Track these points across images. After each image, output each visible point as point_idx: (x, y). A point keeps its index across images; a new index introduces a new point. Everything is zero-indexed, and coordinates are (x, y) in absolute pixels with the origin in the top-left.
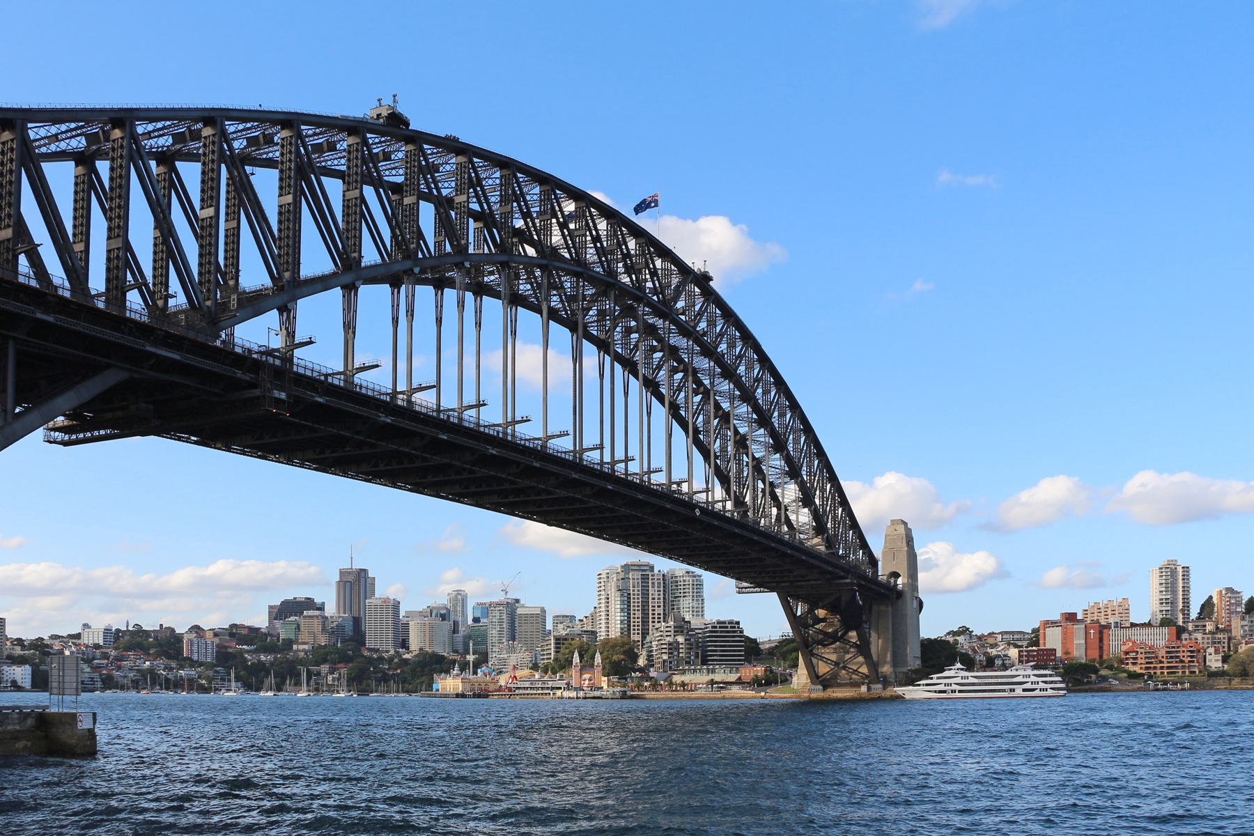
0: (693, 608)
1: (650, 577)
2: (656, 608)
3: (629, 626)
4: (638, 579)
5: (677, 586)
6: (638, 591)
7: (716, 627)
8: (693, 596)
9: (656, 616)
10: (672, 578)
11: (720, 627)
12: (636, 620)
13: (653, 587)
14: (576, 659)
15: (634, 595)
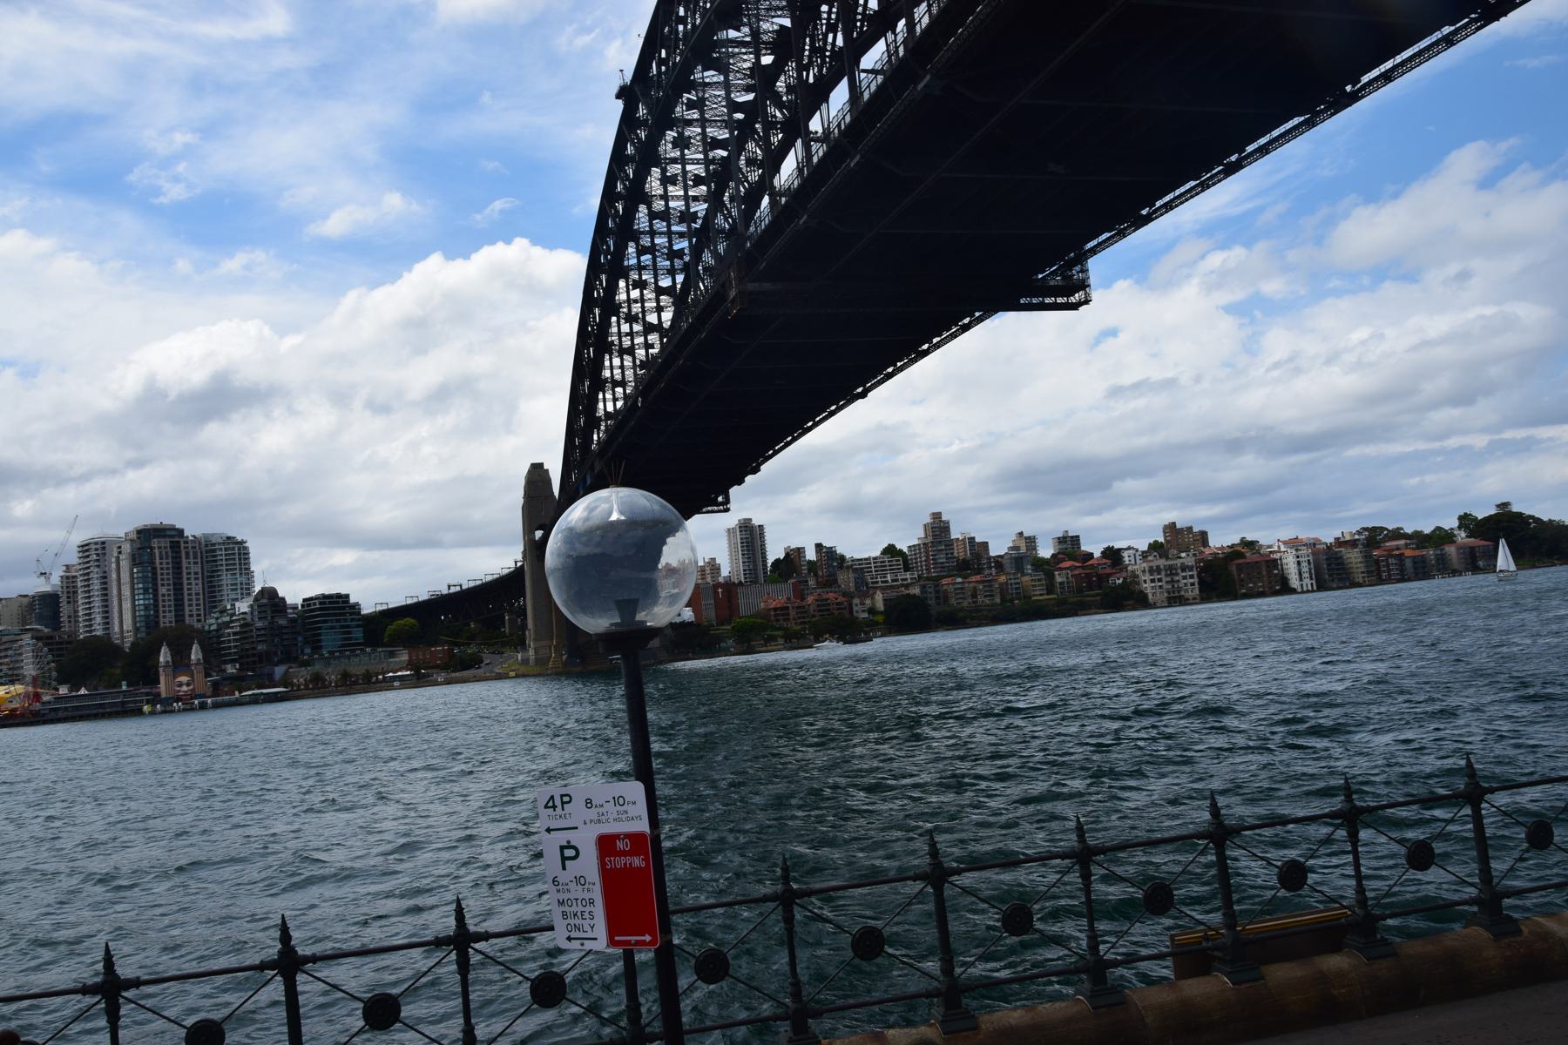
0: (241, 584)
1: (182, 545)
2: (193, 581)
3: (157, 611)
4: (166, 547)
5: (216, 556)
6: (168, 563)
7: (325, 603)
8: (241, 569)
9: (194, 597)
10: (206, 545)
11: (330, 603)
12: (167, 603)
13: (187, 557)
14: (164, 656)
15: (162, 569)
